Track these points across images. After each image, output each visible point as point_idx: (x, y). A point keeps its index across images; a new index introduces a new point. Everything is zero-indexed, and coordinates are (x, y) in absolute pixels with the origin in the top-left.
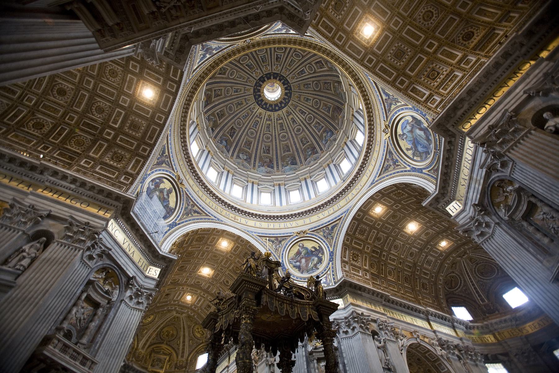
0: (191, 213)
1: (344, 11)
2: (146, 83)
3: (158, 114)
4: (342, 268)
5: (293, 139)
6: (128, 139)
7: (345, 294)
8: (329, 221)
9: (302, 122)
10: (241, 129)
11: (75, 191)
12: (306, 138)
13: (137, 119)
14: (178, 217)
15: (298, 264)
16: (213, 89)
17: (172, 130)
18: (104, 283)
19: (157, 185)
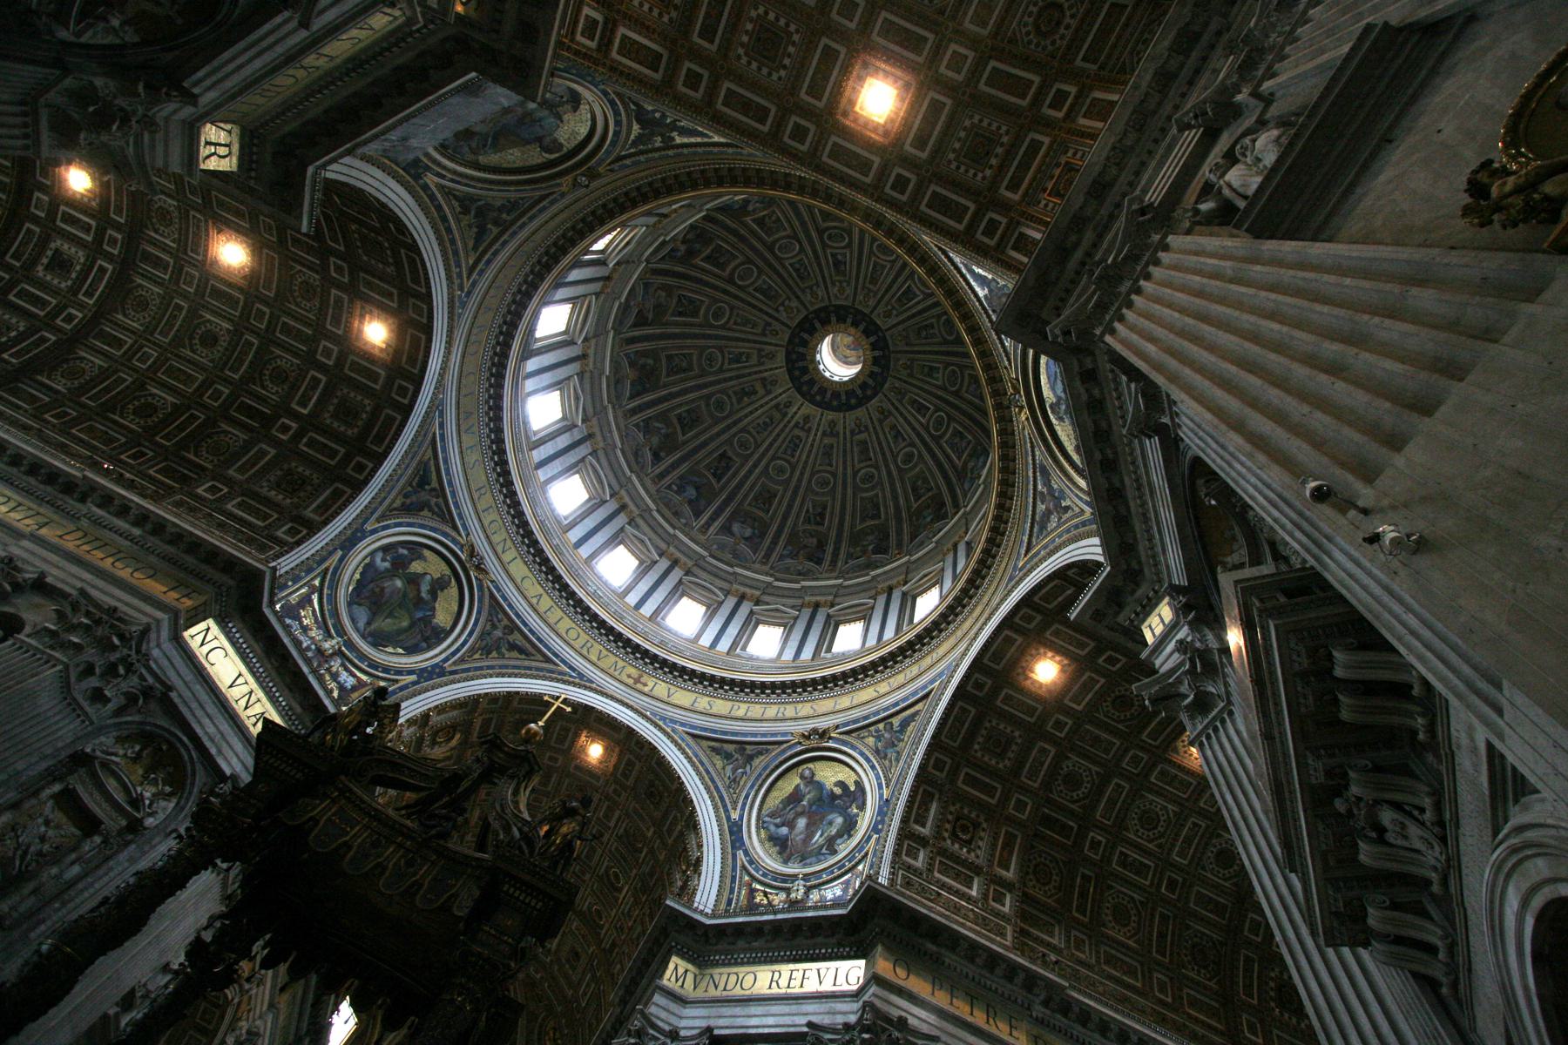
0: (498, 649)
1: (789, 56)
2: (368, 307)
3: (398, 381)
4: (896, 853)
5: (892, 485)
6: (325, 441)
7: (873, 946)
8: (896, 704)
9: (918, 435)
10: (746, 458)
11: (136, 543)
12: (925, 480)
13: (352, 395)
14: (454, 654)
15: (784, 830)
16: (663, 356)
17: (451, 427)
18: (145, 777)
19: (399, 565)
